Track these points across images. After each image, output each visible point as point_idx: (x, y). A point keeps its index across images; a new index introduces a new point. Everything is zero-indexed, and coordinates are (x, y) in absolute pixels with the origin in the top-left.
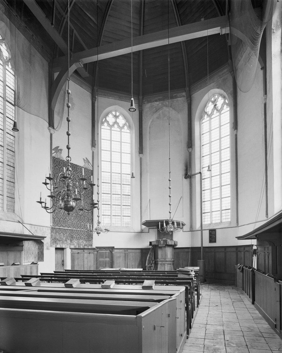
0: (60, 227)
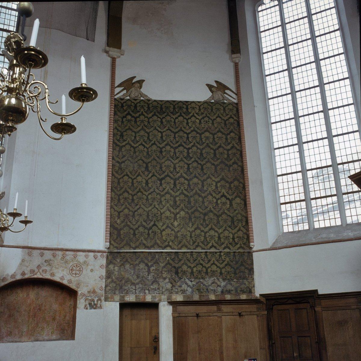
0: (134, 249)
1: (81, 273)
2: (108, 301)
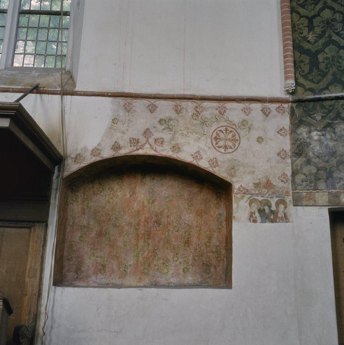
1: (237, 145)
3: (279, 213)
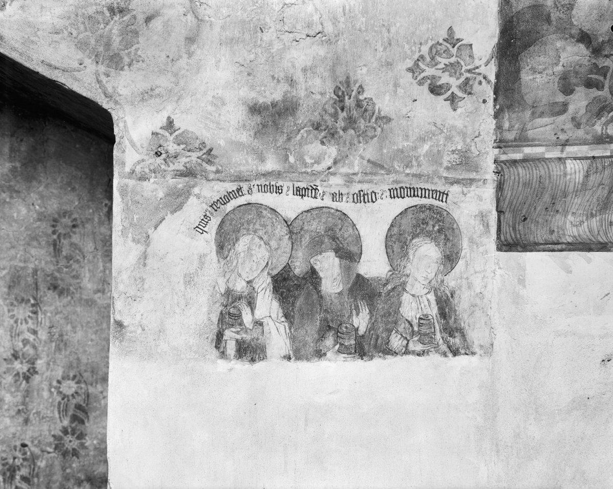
2: (554, 245)
3: (406, 298)
